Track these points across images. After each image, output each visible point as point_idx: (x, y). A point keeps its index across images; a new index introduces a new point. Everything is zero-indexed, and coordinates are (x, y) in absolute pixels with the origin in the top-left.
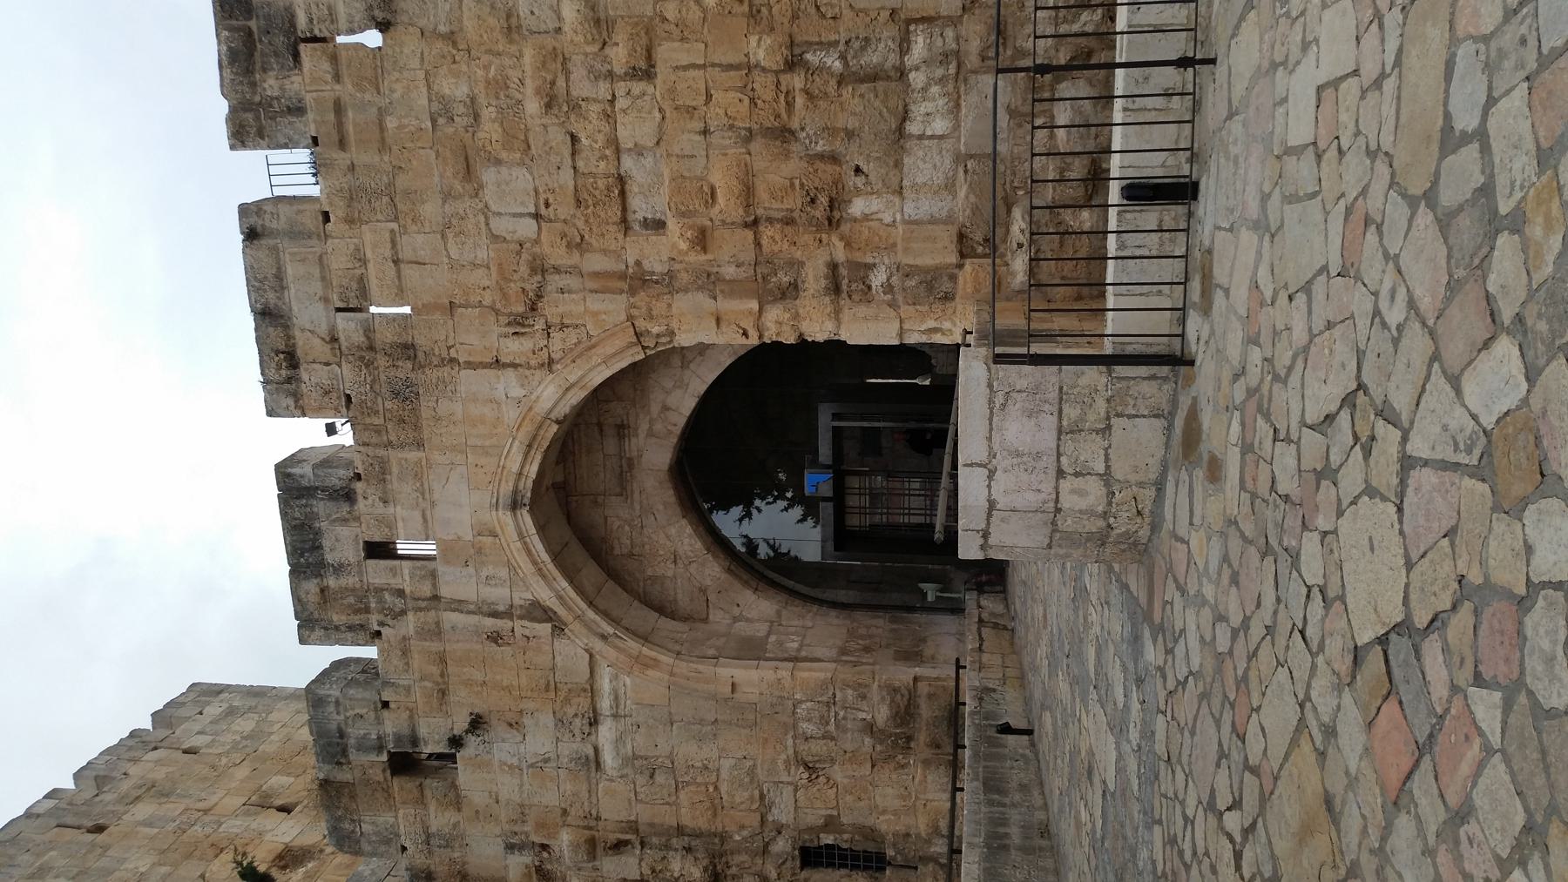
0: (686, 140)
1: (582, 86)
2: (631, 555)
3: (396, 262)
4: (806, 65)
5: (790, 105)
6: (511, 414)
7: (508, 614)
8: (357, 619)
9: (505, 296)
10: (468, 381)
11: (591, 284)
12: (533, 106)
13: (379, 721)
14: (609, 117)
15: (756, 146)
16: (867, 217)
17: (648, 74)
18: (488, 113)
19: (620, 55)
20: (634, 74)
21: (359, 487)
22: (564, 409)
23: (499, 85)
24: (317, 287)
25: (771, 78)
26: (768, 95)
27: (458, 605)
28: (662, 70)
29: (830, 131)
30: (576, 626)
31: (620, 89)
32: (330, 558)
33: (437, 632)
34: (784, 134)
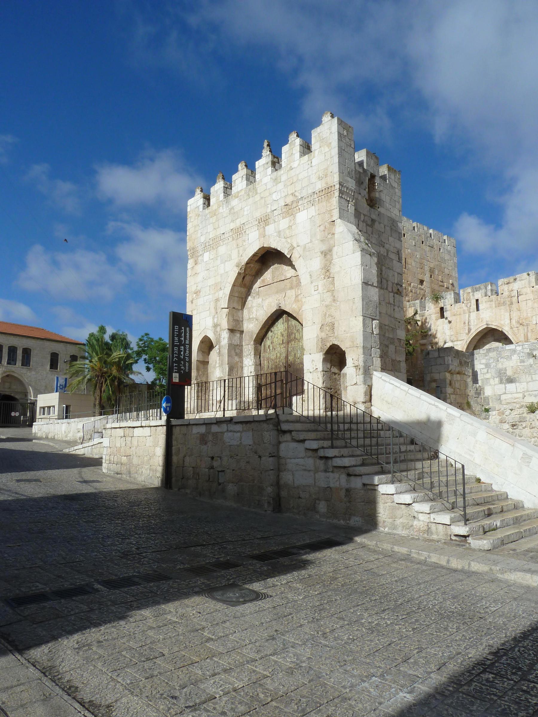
2: (483, 343)
3: (526, 300)
6: (502, 322)
7: (469, 325)
8: (465, 299)
9: (522, 319)
10: (507, 315)
11: (526, 335)
13: (448, 305)
21: (488, 297)
22: (504, 331)
24: (521, 287)
27: (469, 316)
30: (468, 337)
32: (475, 293)
33: (464, 313)
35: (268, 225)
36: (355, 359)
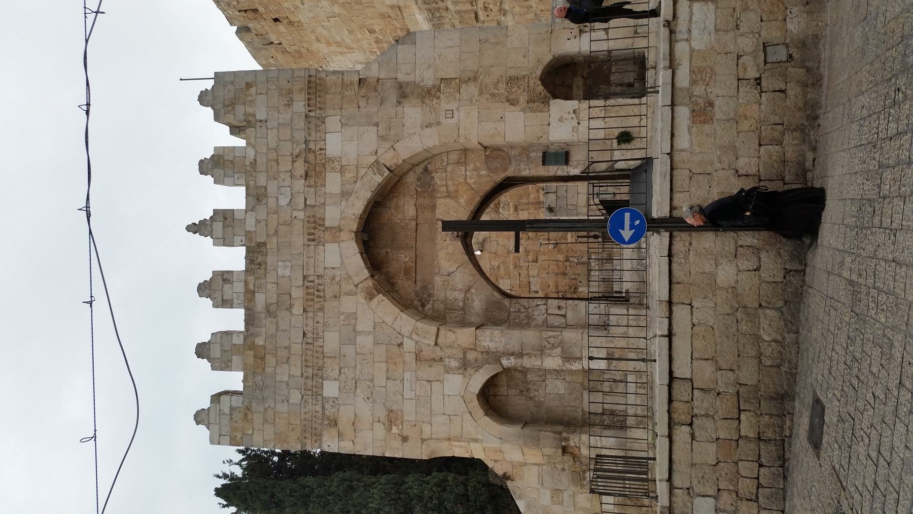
0: (544, 275)
1: (522, 263)
4: (570, 261)
5: (566, 268)
12: (512, 267)
14: (528, 270)
15: (559, 276)
16: (582, 292)
17: (536, 261)
18: (502, 268)
19: (531, 258)
20: (533, 261)
23: (504, 263)
25: (562, 263)
26: (562, 266)
28: (539, 261)
29: (575, 274)
31: (530, 264)
34: (565, 274)
35: (324, 220)
36: (569, 36)
